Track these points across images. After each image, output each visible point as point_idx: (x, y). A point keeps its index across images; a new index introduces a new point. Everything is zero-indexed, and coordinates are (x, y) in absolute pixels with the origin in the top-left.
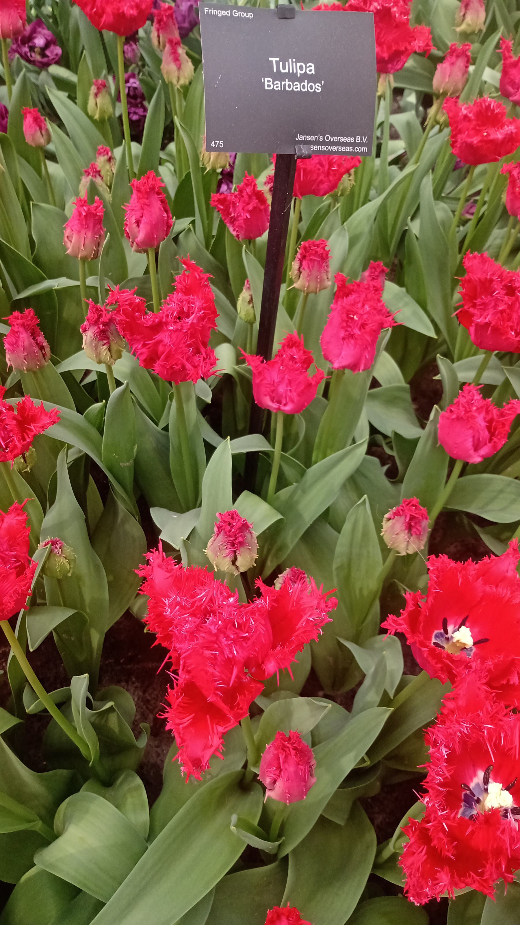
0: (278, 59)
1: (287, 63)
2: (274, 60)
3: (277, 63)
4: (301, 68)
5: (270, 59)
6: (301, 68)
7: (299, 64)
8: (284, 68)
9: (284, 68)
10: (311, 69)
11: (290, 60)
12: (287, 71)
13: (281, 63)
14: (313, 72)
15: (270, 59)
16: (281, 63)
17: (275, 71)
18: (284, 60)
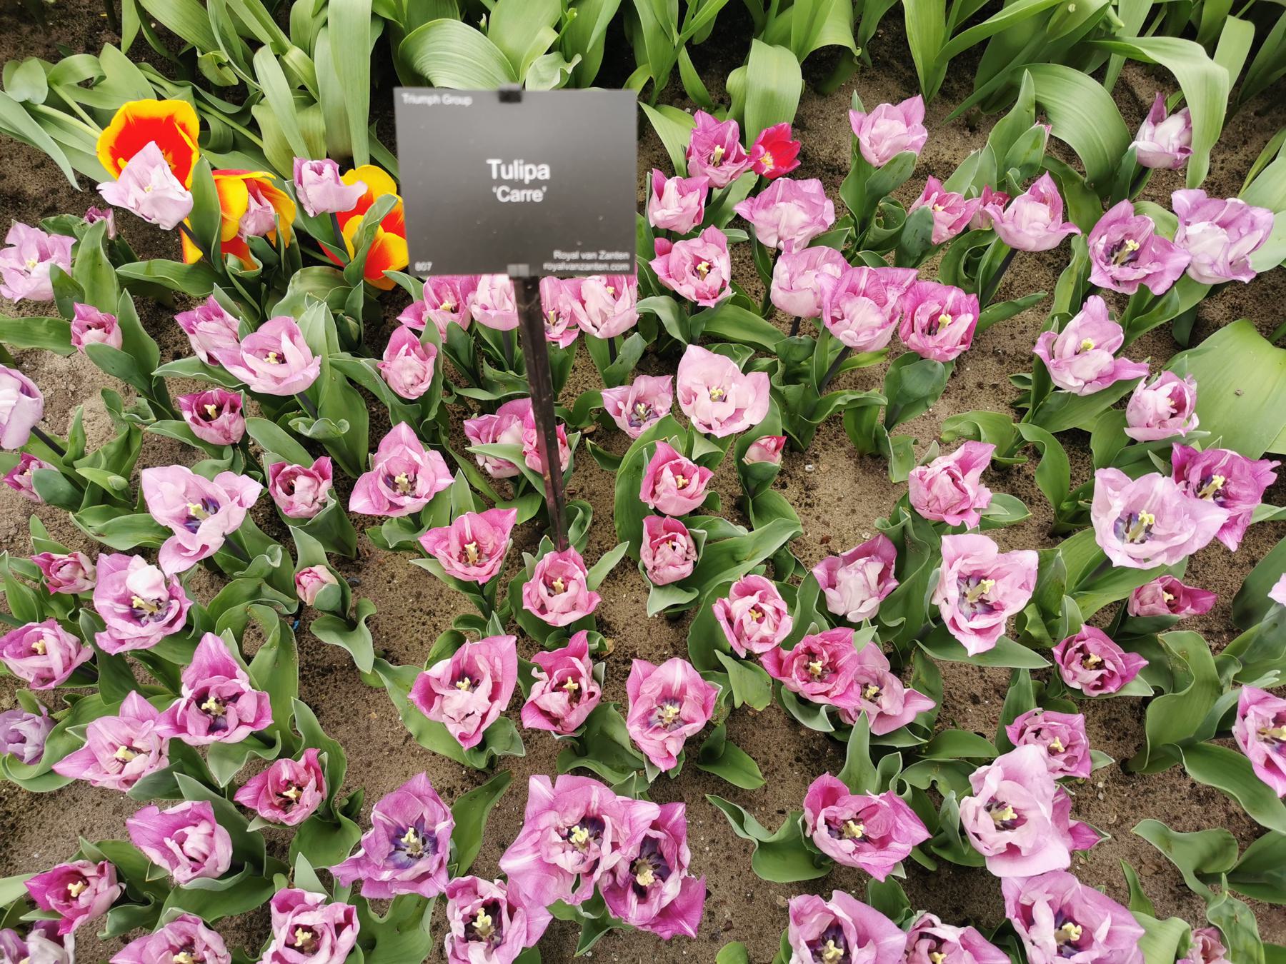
0: (499, 161)
1: (510, 167)
2: (494, 163)
3: (499, 166)
4: (531, 172)
5: (489, 161)
6: (531, 172)
7: (528, 167)
8: (507, 173)
9: (507, 173)
10: (544, 172)
11: (516, 163)
12: (510, 176)
13: (503, 168)
14: (547, 176)
15: (489, 161)
16: (503, 168)
17: (495, 176)
18: (508, 162)
